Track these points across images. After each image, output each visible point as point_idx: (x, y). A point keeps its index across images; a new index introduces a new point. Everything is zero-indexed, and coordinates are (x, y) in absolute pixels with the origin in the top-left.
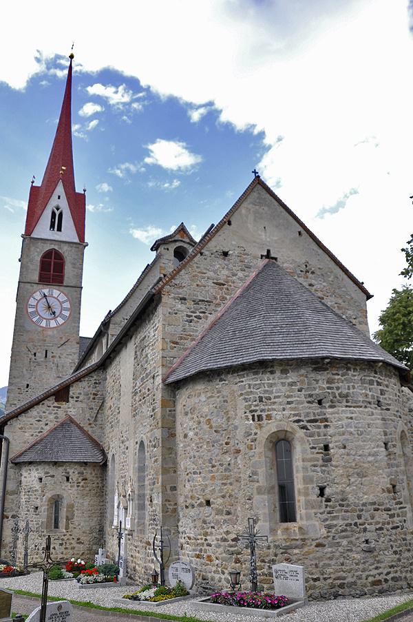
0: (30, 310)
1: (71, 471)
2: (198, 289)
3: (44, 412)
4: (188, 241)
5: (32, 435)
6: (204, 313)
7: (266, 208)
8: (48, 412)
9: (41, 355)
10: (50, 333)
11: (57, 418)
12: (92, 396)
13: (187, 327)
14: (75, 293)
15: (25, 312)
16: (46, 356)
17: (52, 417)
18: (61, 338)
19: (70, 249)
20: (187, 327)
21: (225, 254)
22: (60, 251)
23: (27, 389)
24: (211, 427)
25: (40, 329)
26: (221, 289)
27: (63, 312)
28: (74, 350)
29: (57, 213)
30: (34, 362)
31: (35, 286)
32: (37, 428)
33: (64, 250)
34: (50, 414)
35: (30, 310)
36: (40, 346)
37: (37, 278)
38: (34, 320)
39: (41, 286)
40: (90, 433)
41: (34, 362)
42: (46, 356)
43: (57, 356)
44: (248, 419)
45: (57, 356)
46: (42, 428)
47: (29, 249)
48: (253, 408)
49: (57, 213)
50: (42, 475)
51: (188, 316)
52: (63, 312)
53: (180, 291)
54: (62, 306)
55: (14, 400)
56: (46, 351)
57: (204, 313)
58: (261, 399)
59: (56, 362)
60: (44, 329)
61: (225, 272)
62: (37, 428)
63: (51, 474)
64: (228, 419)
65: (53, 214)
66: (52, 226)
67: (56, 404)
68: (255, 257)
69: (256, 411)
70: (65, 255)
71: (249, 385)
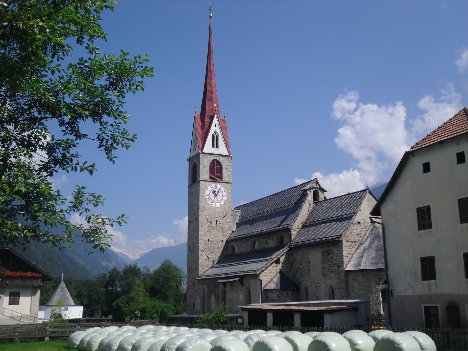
0: (207, 197)
1: (289, 293)
2: (352, 237)
3: (272, 269)
4: (318, 187)
5: (269, 278)
6: (354, 245)
7: (371, 202)
8: (273, 269)
9: (214, 223)
10: (217, 210)
11: (276, 271)
12: (287, 262)
13: (350, 251)
14: (229, 186)
15: (204, 198)
16: (216, 224)
17: (275, 271)
18: (223, 213)
19: (224, 159)
20: (350, 251)
21: (359, 223)
22: (219, 160)
23: (208, 242)
24: (363, 285)
25: (212, 208)
26: (358, 236)
27: (224, 198)
28: (230, 220)
29: (216, 136)
30: (211, 227)
31: (208, 182)
32: (270, 276)
33: (221, 159)
34: (274, 269)
35: (207, 197)
36: (213, 218)
37: (209, 178)
38: (209, 202)
39: (211, 183)
40: (288, 276)
41: (211, 227)
42: (216, 224)
43: (222, 223)
44: (375, 284)
45: (222, 223)
46: (272, 275)
47: (203, 160)
48: (377, 281)
49: (216, 136)
50: (279, 294)
51: (350, 247)
52: (224, 198)
53: (347, 238)
54: (222, 194)
55: (202, 248)
56: (216, 220)
57: (354, 245)
58: (379, 279)
59: (221, 227)
60: (215, 208)
61: (359, 230)
62: (270, 276)
63: (282, 294)
64: (369, 283)
65: (213, 136)
66: (213, 146)
67: (276, 265)
68: (368, 223)
69: (377, 282)
70: (222, 163)
71: (376, 275)
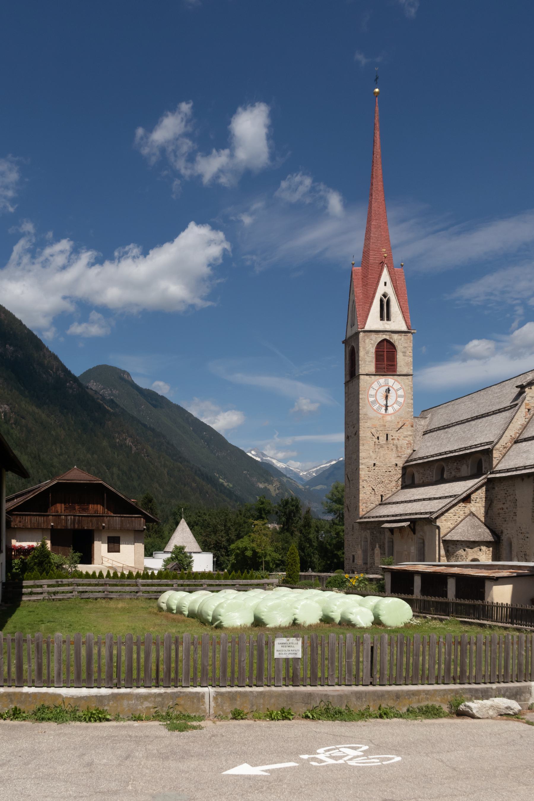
3: (457, 510)
5: (452, 524)
9: (383, 439)
11: (465, 513)
14: (407, 381)
16: (387, 439)
17: (462, 512)
18: (398, 422)
19: (400, 337)
22: (391, 340)
23: (374, 468)
25: (380, 416)
27: (399, 399)
28: (410, 433)
29: (385, 300)
30: (378, 445)
31: (373, 377)
32: (454, 520)
33: (395, 338)
34: (461, 511)
35: (371, 399)
36: (382, 431)
39: (378, 377)
41: (378, 445)
42: (387, 439)
46: (457, 520)
47: (364, 342)
49: (385, 300)
54: (397, 394)
56: (387, 435)
62: (454, 520)
65: (381, 301)
66: (382, 318)
67: (464, 505)
70: (396, 344)
